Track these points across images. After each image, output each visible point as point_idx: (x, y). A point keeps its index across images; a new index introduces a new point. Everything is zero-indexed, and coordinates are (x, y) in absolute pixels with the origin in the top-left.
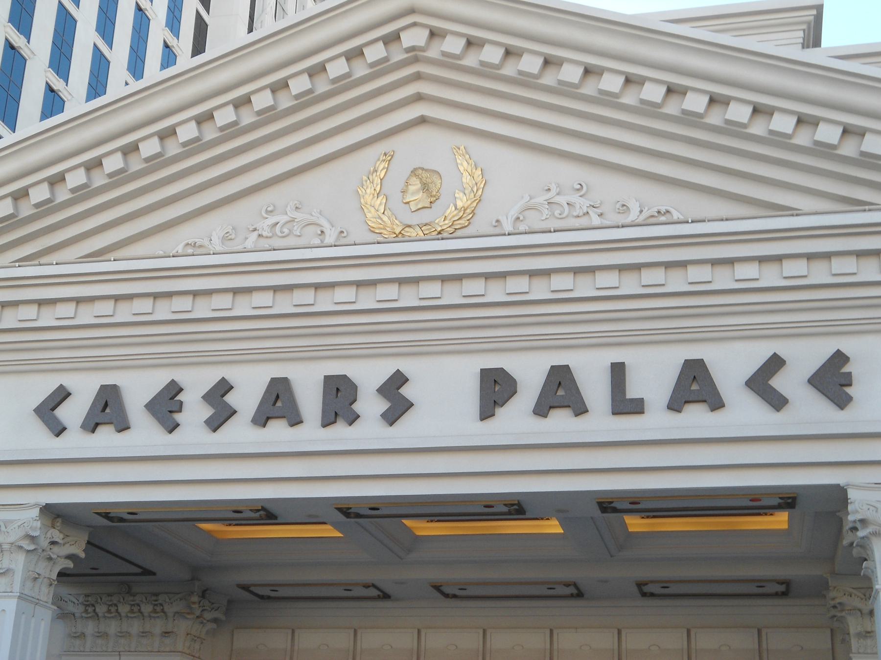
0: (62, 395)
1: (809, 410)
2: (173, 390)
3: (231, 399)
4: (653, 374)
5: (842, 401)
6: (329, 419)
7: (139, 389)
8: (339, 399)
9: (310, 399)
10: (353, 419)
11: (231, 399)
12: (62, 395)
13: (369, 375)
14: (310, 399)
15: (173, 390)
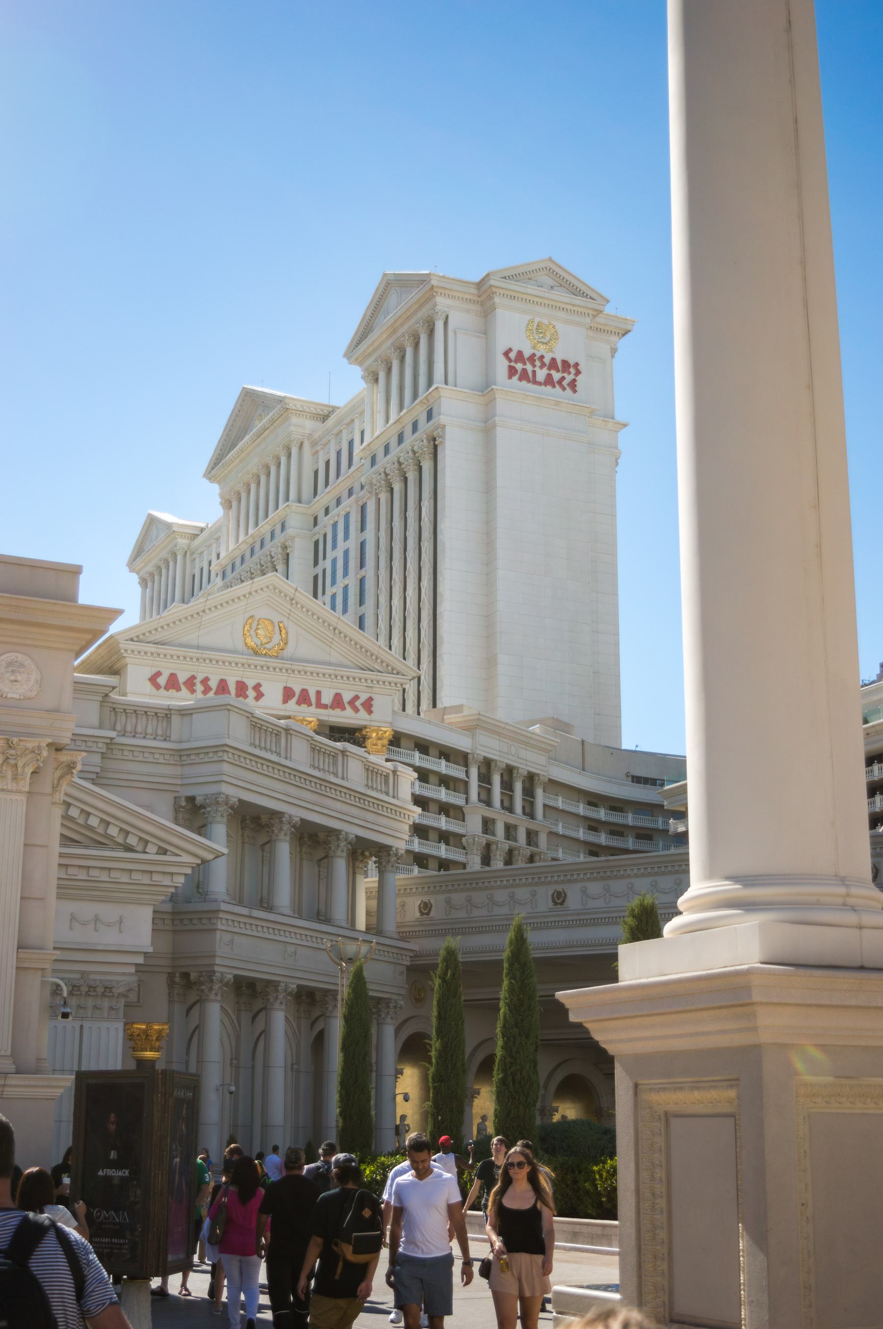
0: (158, 674)
1: (363, 713)
2: (193, 678)
3: (209, 683)
4: (327, 699)
5: (370, 712)
6: (238, 695)
7: (182, 678)
8: (241, 688)
9: (232, 688)
10: (246, 697)
11: (209, 683)
12: (158, 674)
13: (251, 683)
14: (232, 688)
15: (193, 678)
